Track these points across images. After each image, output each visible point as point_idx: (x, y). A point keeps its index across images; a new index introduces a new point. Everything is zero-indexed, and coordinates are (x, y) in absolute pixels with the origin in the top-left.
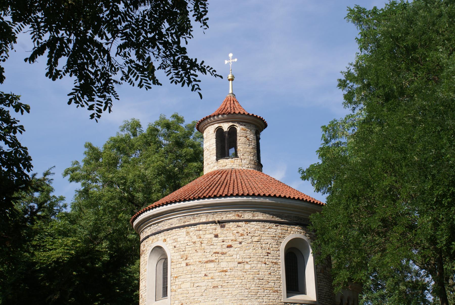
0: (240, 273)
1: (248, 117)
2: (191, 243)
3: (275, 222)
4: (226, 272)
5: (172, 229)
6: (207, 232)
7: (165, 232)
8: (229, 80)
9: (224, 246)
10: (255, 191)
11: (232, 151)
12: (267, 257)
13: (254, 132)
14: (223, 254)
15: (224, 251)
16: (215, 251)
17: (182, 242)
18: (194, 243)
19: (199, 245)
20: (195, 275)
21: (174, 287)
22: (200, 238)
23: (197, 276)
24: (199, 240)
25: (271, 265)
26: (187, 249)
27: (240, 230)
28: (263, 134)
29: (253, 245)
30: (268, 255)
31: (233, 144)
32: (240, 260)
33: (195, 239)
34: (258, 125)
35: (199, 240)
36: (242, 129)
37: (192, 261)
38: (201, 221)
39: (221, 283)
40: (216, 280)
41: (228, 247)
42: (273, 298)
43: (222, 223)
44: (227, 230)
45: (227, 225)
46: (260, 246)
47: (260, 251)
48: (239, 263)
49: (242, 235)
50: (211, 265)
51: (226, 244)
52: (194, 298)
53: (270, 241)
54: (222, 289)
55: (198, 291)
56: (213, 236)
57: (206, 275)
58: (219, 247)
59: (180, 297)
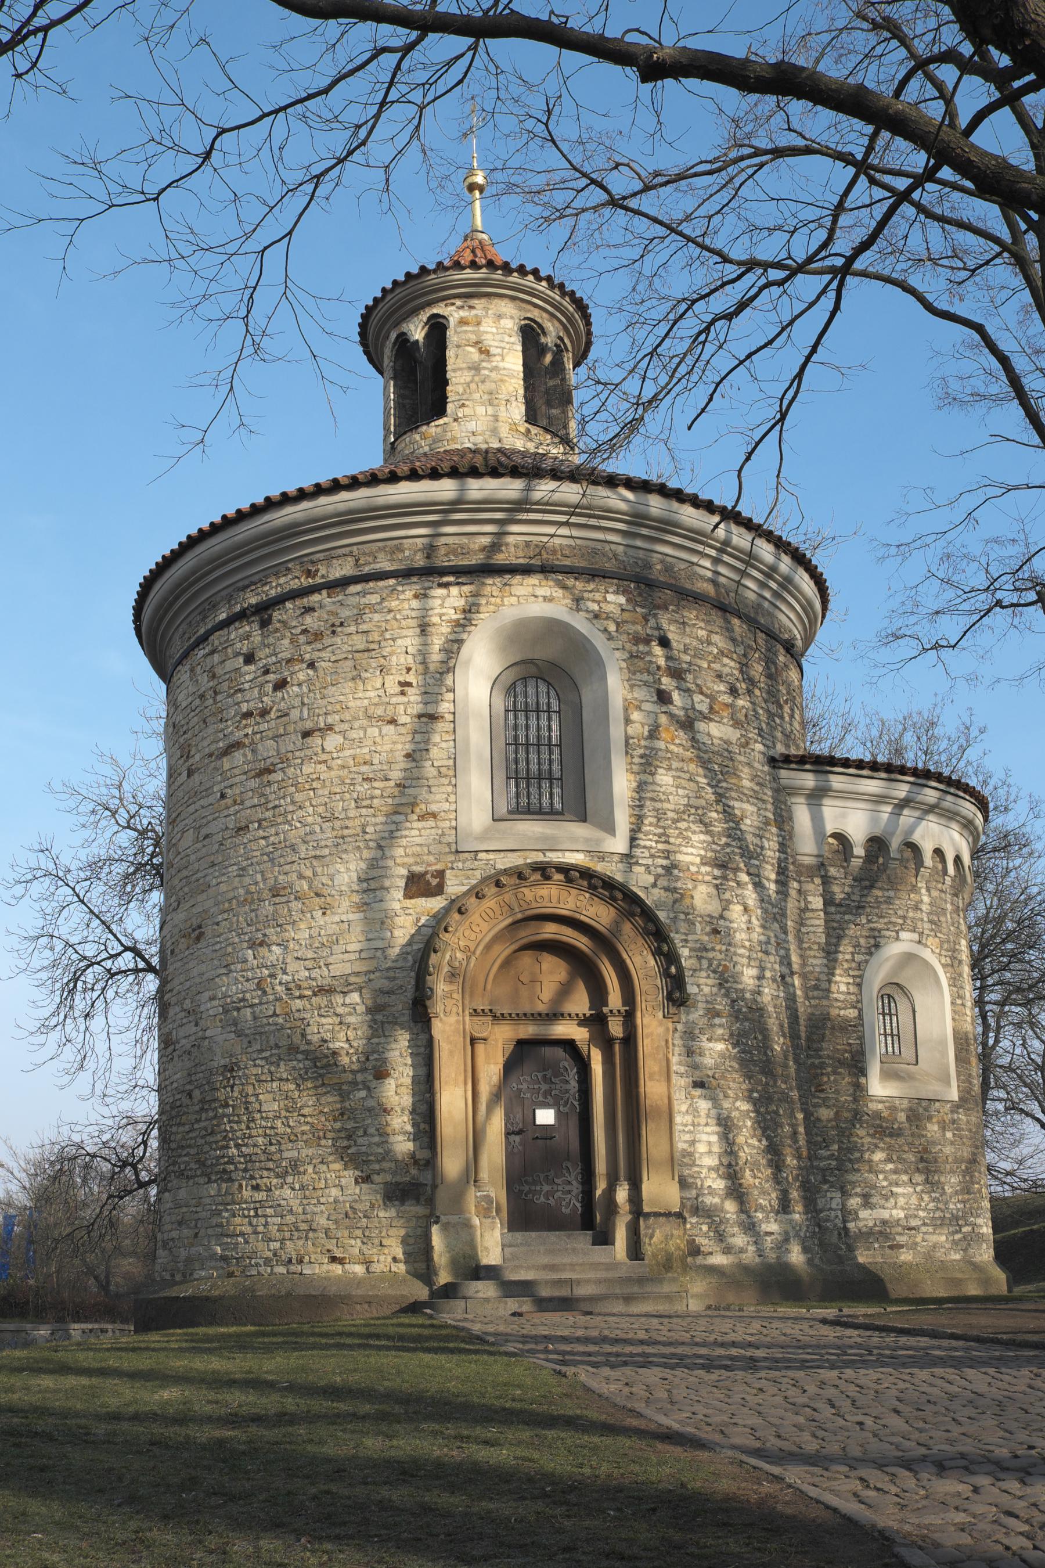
2: (197, 702)
4: (268, 771)
6: (229, 650)
12: (404, 699)
14: (264, 713)
16: (244, 707)
17: (184, 704)
18: (202, 697)
19: (211, 701)
20: (202, 802)
22: (214, 676)
23: (204, 802)
24: (211, 684)
26: (191, 725)
30: (403, 693)
32: (309, 725)
35: (211, 684)
37: (197, 757)
38: (217, 620)
40: (248, 804)
42: (419, 840)
44: (277, 630)
52: (199, 875)
54: (261, 833)
55: (204, 850)
56: (241, 659)
57: (223, 796)
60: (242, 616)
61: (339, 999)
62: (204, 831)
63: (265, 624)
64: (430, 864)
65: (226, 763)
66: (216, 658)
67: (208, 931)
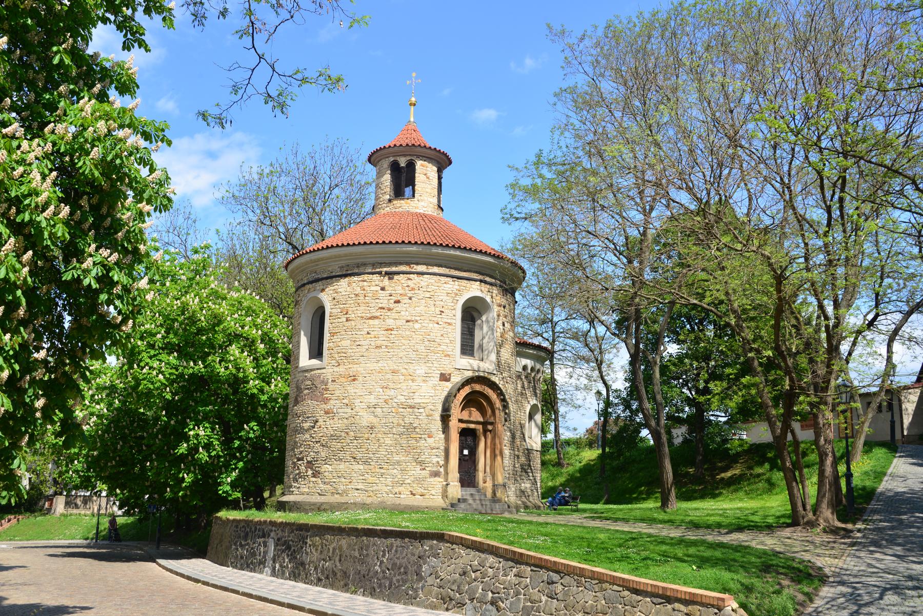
0: (408, 333)
1: (429, 151)
3: (453, 277)
5: (332, 277)
7: (324, 282)
8: (411, 104)
9: (392, 301)
10: (433, 239)
11: (408, 191)
13: (435, 169)
14: (389, 310)
15: (391, 306)
16: (380, 305)
18: (356, 295)
21: (331, 344)
25: (445, 325)
27: (410, 282)
28: (446, 173)
29: (423, 301)
31: (411, 182)
32: (409, 318)
33: (358, 290)
34: (442, 161)
36: (422, 165)
39: (385, 343)
41: (395, 302)
43: (390, 275)
45: (396, 277)
46: (432, 303)
47: (433, 309)
48: (408, 321)
49: (413, 289)
50: (376, 322)
51: (394, 298)
53: (445, 298)
58: (386, 301)
59: (336, 356)
60: (380, 273)
61: (416, 410)
62: (358, 343)
63: (392, 279)
64: (447, 370)
65: (371, 322)
66: (365, 283)
67: (360, 379)
